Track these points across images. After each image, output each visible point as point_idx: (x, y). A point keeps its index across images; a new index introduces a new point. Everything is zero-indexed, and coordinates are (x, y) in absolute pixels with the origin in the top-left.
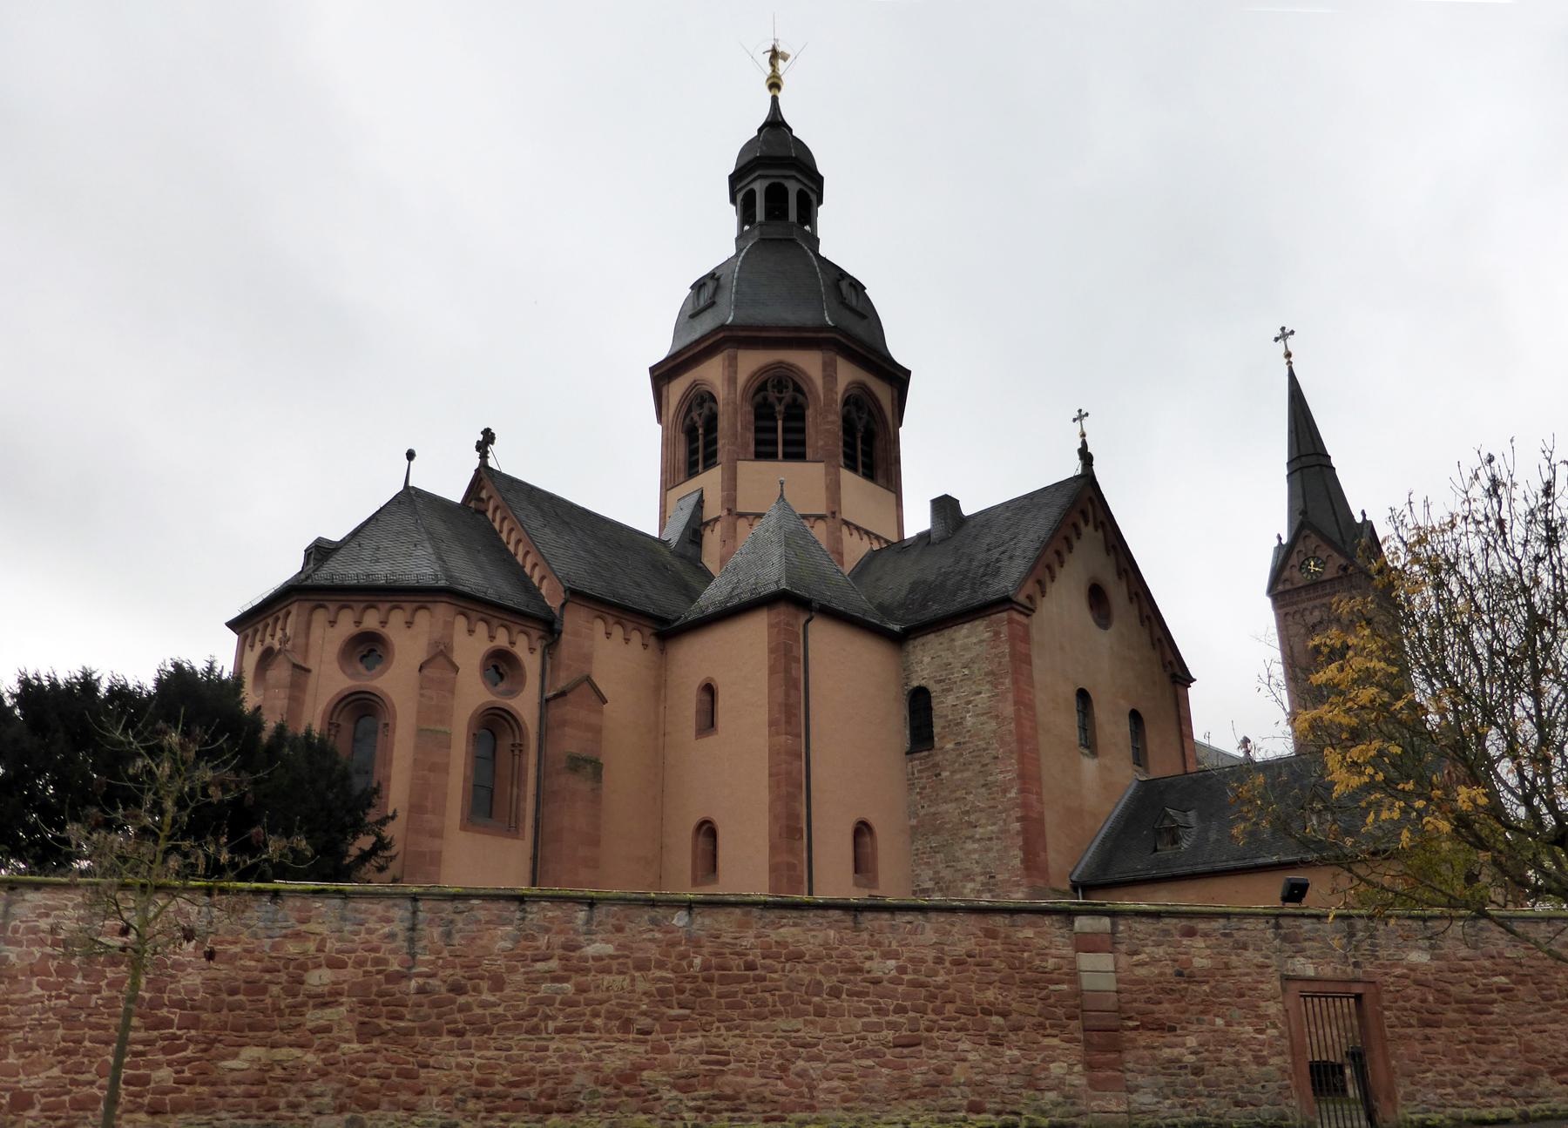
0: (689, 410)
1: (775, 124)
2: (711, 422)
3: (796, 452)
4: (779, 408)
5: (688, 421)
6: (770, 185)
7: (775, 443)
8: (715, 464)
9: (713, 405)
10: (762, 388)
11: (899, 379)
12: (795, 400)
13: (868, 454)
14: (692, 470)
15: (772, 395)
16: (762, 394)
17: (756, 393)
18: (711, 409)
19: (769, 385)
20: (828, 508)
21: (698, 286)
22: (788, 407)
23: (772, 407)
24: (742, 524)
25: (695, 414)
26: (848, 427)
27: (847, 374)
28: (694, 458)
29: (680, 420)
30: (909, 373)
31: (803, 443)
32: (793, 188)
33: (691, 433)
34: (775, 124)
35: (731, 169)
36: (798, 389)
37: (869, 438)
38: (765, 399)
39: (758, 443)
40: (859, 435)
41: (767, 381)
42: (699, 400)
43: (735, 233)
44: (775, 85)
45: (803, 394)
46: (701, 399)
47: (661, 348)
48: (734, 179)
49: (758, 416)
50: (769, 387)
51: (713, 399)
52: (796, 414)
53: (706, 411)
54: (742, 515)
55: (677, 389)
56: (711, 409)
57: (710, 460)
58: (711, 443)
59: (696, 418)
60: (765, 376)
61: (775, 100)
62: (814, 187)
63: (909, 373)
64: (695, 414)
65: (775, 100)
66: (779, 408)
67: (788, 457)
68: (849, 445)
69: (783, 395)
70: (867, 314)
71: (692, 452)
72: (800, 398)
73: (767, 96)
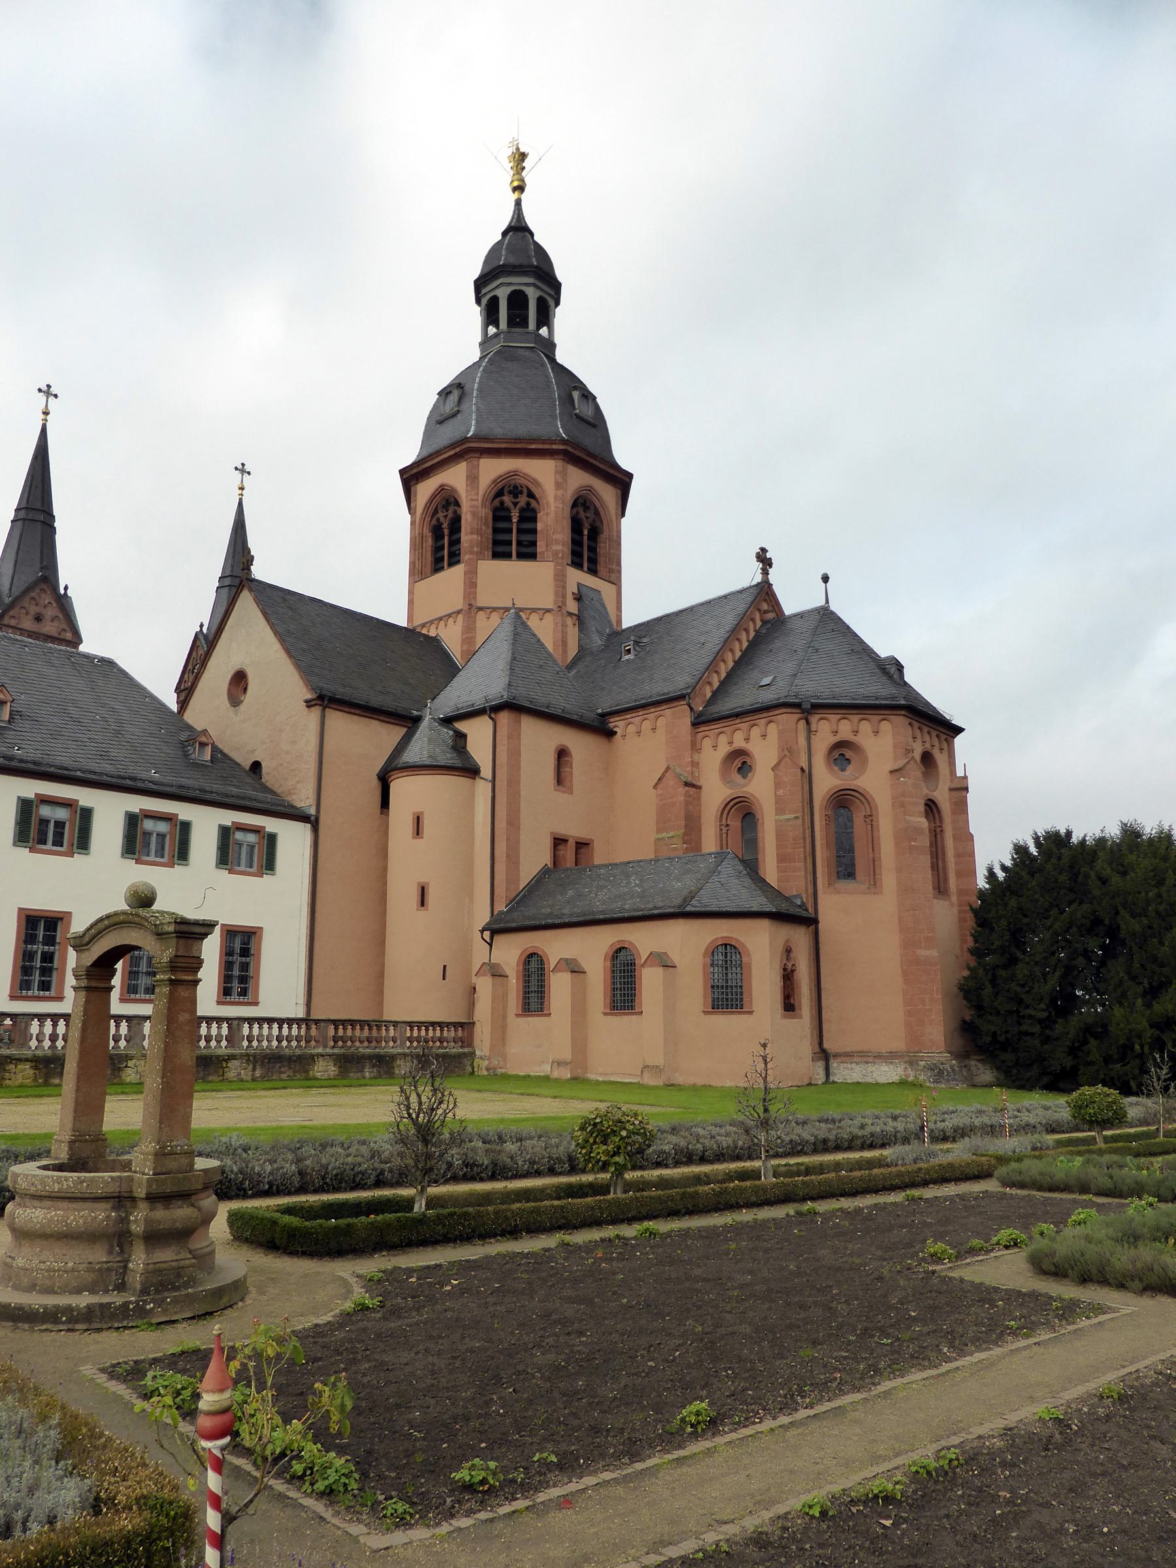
0: (436, 512)
1: (518, 229)
2: (456, 524)
3: (528, 553)
5: (434, 522)
7: (510, 543)
8: (458, 562)
9: (456, 508)
10: (500, 493)
11: (622, 481)
12: (528, 504)
13: (593, 550)
14: (437, 566)
15: (507, 499)
16: (498, 499)
18: (455, 512)
19: (506, 491)
21: (445, 393)
22: (522, 510)
23: (508, 510)
26: (576, 525)
27: (578, 478)
28: (439, 555)
29: (428, 519)
30: (630, 476)
31: (534, 544)
32: (532, 294)
33: (437, 532)
34: (518, 229)
35: (476, 274)
36: (531, 495)
37: (595, 533)
38: (502, 503)
39: (496, 543)
40: (586, 532)
41: (503, 489)
42: (444, 503)
43: (478, 338)
46: (447, 501)
47: (409, 454)
48: (479, 284)
49: (496, 518)
50: (506, 493)
51: (457, 504)
52: (529, 516)
53: (450, 514)
54: (480, 609)
55: (425, 489)
56: (455, 512)
57: (455, 559)
58: (455, 542)
59: (442, 519)
60: (500, 486)
61: (518, 203)
62: (553, 293)
63: (630, 476)
64: (441, 515)
65: (518, 203)
67: (522, 556)
68: (576, 542)
70: (596, 423)
71: (438, 549)
72: (533, 504)
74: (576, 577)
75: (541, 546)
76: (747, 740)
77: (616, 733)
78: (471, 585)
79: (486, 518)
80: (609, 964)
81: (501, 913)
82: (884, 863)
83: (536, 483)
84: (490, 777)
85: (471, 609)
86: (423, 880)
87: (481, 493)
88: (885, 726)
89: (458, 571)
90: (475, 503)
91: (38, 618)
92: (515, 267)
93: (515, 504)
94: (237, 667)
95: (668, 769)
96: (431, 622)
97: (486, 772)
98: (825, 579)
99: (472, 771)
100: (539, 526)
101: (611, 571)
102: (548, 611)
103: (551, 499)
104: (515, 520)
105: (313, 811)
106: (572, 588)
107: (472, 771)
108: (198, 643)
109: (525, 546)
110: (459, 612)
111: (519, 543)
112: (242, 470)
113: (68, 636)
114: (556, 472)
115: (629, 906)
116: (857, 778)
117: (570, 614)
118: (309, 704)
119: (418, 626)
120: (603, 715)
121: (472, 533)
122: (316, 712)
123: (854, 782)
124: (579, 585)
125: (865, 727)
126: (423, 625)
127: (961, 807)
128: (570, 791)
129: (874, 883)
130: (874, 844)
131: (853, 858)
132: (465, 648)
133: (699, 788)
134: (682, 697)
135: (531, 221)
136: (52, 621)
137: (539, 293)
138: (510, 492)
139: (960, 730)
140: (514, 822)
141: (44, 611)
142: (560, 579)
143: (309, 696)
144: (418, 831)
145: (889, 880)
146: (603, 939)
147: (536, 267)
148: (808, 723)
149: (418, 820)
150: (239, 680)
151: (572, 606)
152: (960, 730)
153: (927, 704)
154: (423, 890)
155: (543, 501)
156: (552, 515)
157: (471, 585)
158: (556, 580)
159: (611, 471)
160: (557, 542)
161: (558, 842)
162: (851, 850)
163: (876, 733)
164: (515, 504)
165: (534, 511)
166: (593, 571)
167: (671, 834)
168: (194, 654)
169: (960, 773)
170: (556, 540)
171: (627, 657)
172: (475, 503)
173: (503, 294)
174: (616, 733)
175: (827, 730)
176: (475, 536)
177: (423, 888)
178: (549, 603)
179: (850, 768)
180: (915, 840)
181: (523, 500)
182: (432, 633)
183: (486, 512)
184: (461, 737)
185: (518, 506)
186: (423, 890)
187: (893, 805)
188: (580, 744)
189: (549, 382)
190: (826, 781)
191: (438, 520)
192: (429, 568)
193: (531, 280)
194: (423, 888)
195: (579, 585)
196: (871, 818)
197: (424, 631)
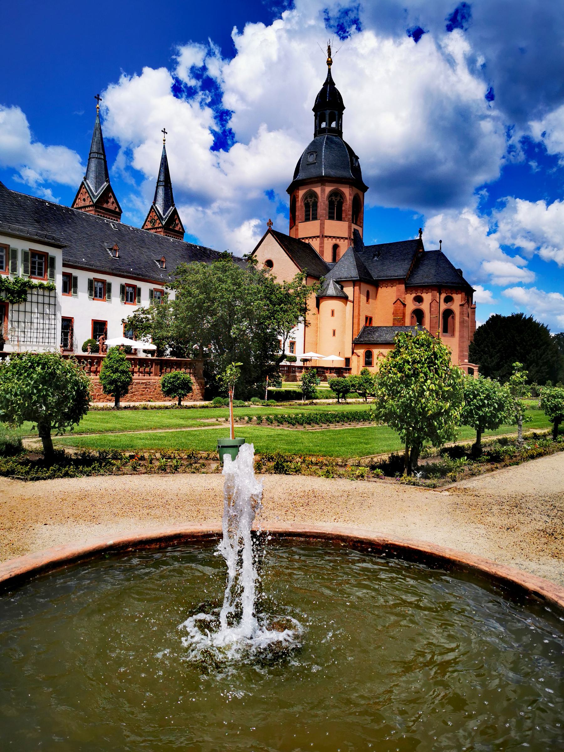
0: (306, 198)
1: (329, 83)
2: (315, 204)
3: (339, 218)
4: (336, 203)
5: (306, 202)
12: (340, 200)
18: (315, 200)
24: (326, 239)
25: (309, 200)
33: (307, 206)
38: (332, 199)
44: (329, 63)
54: (326, 237)
61: (329, 70)
65: (329, 70)
72: (342, 200)
73: (327, 67)
74: (354, 226)
75: (344, 215)
81: (356, 338)
85: (322, 237)
86: (334, 329)
89: (317, 223)
93: (336, 200)
94: (268, 258)
95: (398, 299)
96: (307, 238)
97: (351, 298)
98: (441, 242)
99: (344, 298)
101: (361, 222)
102: (346, 238)
103: (348, 199)
106: (353, 230)
110: (318, 237)
112: (164, 132)
113: (117, 210)
124: (355, 229)
126: (303, 238)
129: (453, 335)
135: (339, 86)
140: (359, 314)
142: (350, 227)
144: (333, 314)
145: (457, 333)
149: (333, 312)
150: (269, 263)
151: (352, 237)
160: (349, 215)
166: (356, 224)
168: (151, 214)
169: (474, 303)
176: (324, 211)
181: (338, 198)
182: (307, 241)
183: (327, 202)
187: (460, 314)
188: (371, 289)
190: (443, 306)
191: (307, 201)
192: (304, 219)
195: (355, 229)
196: (453, 318)
197: (303, 241)
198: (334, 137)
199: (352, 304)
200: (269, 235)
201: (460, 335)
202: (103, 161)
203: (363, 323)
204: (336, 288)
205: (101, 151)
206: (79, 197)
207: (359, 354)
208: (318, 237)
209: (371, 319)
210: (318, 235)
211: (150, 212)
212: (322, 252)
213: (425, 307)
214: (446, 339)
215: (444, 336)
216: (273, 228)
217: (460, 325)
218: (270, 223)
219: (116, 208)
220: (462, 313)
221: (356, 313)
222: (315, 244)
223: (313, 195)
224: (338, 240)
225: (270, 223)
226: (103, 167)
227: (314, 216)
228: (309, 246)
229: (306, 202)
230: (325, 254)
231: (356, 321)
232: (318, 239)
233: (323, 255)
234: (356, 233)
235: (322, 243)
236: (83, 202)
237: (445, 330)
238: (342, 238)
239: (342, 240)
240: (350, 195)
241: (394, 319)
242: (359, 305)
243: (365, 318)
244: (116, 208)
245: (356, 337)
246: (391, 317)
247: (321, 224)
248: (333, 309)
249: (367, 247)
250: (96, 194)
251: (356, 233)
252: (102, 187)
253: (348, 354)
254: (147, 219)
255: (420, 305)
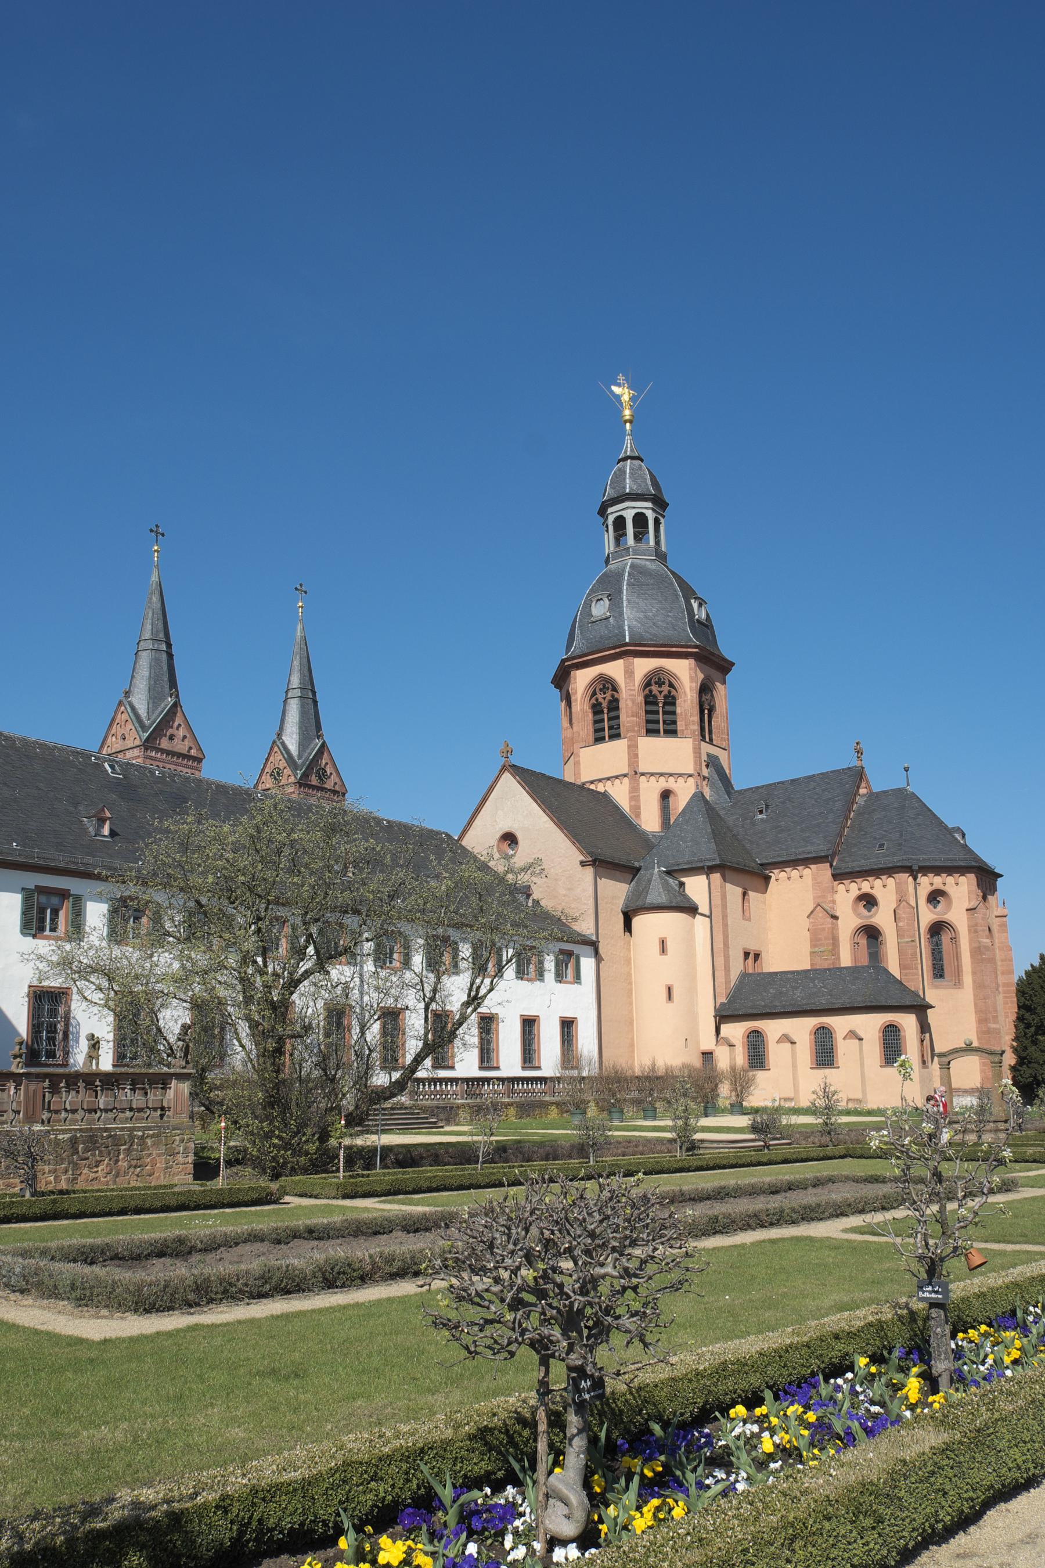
0: (594, 694)
2: (614, 705)
3: (671, 732)
4: (661, 699)
6: (637, 514)
10: (648, 684)
12: (670, 692)
15: (655, 689)
17: (644, 690)
18: (613, 696)
19: (653, 682)
20: (695, 770)
22: (665, 697)
23: (655, 697)
31: (674, 722)
32: (650, 515)
33: (597, 709)
36: (671, 685)
38: (651, 691)
39: (648, 722)
45: (676, 689)
49: (647, 703)
51: (615, 689)
52: (671, 701)
53: (608, 696)
54: (643, 774)
56: (613, 696)
59: (601, 700)
63: (734, 664)
66: (661, 699)
69: (662, 689)
72: (673, 692)
74: (706, 748)
75: (680, 725)
76: (872, 888)
77: (771, 877)
78: (633, 755)
79: (641, 703)
80: (813, 1037)
81: (722, 1004)
82: (964, 969)
83: (675, 676)
84: (707, 913)
85: (635, 774)
86: (669, 983)
87: (637, 684)
88: (963, 879)
89: (621, 745)
90: (632, 692)
91: (171, 738)
92: (637, 494)
93: (661, 692)
94: (506, 829)
96: (600, 780)
97: (703, 908)
98: (906, 770)
99: (692, 910)
100: (679, 710)
102: (690, 776)
103: (688, 690)
104: (661, 705)
105: (594, 938)
106: (704, 757)
107: (692, 910)
108: (276, 749)
109: (668, 724)
110: (625, 775)
111: (664, 722)
113: (193, 752)
114: (690, 669)
115: (823, 1002)
116: (946, 914)
117: (704, 778)
118: (583, 864)
119: (587, 782)
120: (761, 865)
121: (633, 716)
122: (590, 871)
123: (945, 916)
124: (708, 755)
125: (950, 880)
126: (592, 782)
127: (1003, 926)
128: (749, 919)
129: (958, 983)
130: (958, 956)
131: (942, 965)
132: (633, 803)
133: (835, 918)
134: (826, 857)
136: (183, 741)
137: (655, 515)
138: (656, 683)
139: (1001, 876)
141: (175, 732)
142: (697, 751)
143: (582, 858)
144: (663, 950)
145: (968, 979)
146: (811, 1023)
147: (654, 495)
148: (915, 879)
149: (663, 942)
152: (1001, 876)
153: (986, 864)
154: (669, 989)
155: (679, 690)
156: (689, 702)
157: (633, 755)
158: (694, 752)
159: (722, 663)
161: (747, 955)
162: (941, 959)
163: (957, 884)
164: (661, 692)
165: (674, 698)
167: (822, 949)
168: (271, 759)
170: (693, 721)
171: (760, 816)
172: (632, 692)
173: (629, 515)
174: (771, 877)
175: (927, 883)
177: (669, 988)
178: (690, 769)
179: (940, 907)
180: (985, 954)
181: (665, 688)
182: (600, 788)
183: (640, 699)
184: (682, 884)
185: (663, 694)
186: (669, 989)
187: (969, 931)
189: (677, 595)
190: (927, 916)
191: (597, 700)
192: (591, 738)
193: (649, 505)
194: (669, 988)
195: (708, 755)
196: (954, 940)
197: (592, 787)
198: (648, 563)
199: (708, 920)
200: (507, 776)
201: (974, 981)
202: (164, 656)
203: (737, 966)
204: (666, 886)
205: (162, 636)
206: (113, 731)
207: (734, 1041)
208: (625, 775)
209: (757, 956)
210: (625, 771)
211: (269, 754)
212: (637, 809)
213: (883, 918)
214: (942, 992)
215: (936, 987)
216: (515, 760)
217: (972, 956)
218: (508, 752)
219: (190, 748)
220: (973, 929)
221: (719, 945)
222: (620, 793)
223: (606, 684)
224: (671, 779)
225: (508, 752)
226: (165, 668)
227: (613, 732)
228: (605, 795)
229: (593, 701)
230: (644, 815)
231: (720, 961)
232: (626, 780)
233: (638, 815)
234: (713, 762)
235: (634, 791)
236: (120, 741)
237: (939, 972)
238: (680, 775)
239: (681, 780)
240: (692, 679)
241: (812, 953)
242: (725, 925)
243: (742, 955)
244: (190, 748)
245: (722, 999)
246: (806, 949)
247: (629, 747)
248: (663, 936)
249: (740, 792)
250: (147, 723)
251: (713, 762)
252: (160, 709)
253: (707, 1042)
254: (263, 770)
255: (871, 917)
